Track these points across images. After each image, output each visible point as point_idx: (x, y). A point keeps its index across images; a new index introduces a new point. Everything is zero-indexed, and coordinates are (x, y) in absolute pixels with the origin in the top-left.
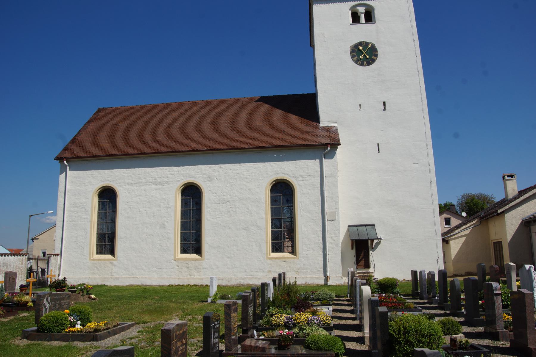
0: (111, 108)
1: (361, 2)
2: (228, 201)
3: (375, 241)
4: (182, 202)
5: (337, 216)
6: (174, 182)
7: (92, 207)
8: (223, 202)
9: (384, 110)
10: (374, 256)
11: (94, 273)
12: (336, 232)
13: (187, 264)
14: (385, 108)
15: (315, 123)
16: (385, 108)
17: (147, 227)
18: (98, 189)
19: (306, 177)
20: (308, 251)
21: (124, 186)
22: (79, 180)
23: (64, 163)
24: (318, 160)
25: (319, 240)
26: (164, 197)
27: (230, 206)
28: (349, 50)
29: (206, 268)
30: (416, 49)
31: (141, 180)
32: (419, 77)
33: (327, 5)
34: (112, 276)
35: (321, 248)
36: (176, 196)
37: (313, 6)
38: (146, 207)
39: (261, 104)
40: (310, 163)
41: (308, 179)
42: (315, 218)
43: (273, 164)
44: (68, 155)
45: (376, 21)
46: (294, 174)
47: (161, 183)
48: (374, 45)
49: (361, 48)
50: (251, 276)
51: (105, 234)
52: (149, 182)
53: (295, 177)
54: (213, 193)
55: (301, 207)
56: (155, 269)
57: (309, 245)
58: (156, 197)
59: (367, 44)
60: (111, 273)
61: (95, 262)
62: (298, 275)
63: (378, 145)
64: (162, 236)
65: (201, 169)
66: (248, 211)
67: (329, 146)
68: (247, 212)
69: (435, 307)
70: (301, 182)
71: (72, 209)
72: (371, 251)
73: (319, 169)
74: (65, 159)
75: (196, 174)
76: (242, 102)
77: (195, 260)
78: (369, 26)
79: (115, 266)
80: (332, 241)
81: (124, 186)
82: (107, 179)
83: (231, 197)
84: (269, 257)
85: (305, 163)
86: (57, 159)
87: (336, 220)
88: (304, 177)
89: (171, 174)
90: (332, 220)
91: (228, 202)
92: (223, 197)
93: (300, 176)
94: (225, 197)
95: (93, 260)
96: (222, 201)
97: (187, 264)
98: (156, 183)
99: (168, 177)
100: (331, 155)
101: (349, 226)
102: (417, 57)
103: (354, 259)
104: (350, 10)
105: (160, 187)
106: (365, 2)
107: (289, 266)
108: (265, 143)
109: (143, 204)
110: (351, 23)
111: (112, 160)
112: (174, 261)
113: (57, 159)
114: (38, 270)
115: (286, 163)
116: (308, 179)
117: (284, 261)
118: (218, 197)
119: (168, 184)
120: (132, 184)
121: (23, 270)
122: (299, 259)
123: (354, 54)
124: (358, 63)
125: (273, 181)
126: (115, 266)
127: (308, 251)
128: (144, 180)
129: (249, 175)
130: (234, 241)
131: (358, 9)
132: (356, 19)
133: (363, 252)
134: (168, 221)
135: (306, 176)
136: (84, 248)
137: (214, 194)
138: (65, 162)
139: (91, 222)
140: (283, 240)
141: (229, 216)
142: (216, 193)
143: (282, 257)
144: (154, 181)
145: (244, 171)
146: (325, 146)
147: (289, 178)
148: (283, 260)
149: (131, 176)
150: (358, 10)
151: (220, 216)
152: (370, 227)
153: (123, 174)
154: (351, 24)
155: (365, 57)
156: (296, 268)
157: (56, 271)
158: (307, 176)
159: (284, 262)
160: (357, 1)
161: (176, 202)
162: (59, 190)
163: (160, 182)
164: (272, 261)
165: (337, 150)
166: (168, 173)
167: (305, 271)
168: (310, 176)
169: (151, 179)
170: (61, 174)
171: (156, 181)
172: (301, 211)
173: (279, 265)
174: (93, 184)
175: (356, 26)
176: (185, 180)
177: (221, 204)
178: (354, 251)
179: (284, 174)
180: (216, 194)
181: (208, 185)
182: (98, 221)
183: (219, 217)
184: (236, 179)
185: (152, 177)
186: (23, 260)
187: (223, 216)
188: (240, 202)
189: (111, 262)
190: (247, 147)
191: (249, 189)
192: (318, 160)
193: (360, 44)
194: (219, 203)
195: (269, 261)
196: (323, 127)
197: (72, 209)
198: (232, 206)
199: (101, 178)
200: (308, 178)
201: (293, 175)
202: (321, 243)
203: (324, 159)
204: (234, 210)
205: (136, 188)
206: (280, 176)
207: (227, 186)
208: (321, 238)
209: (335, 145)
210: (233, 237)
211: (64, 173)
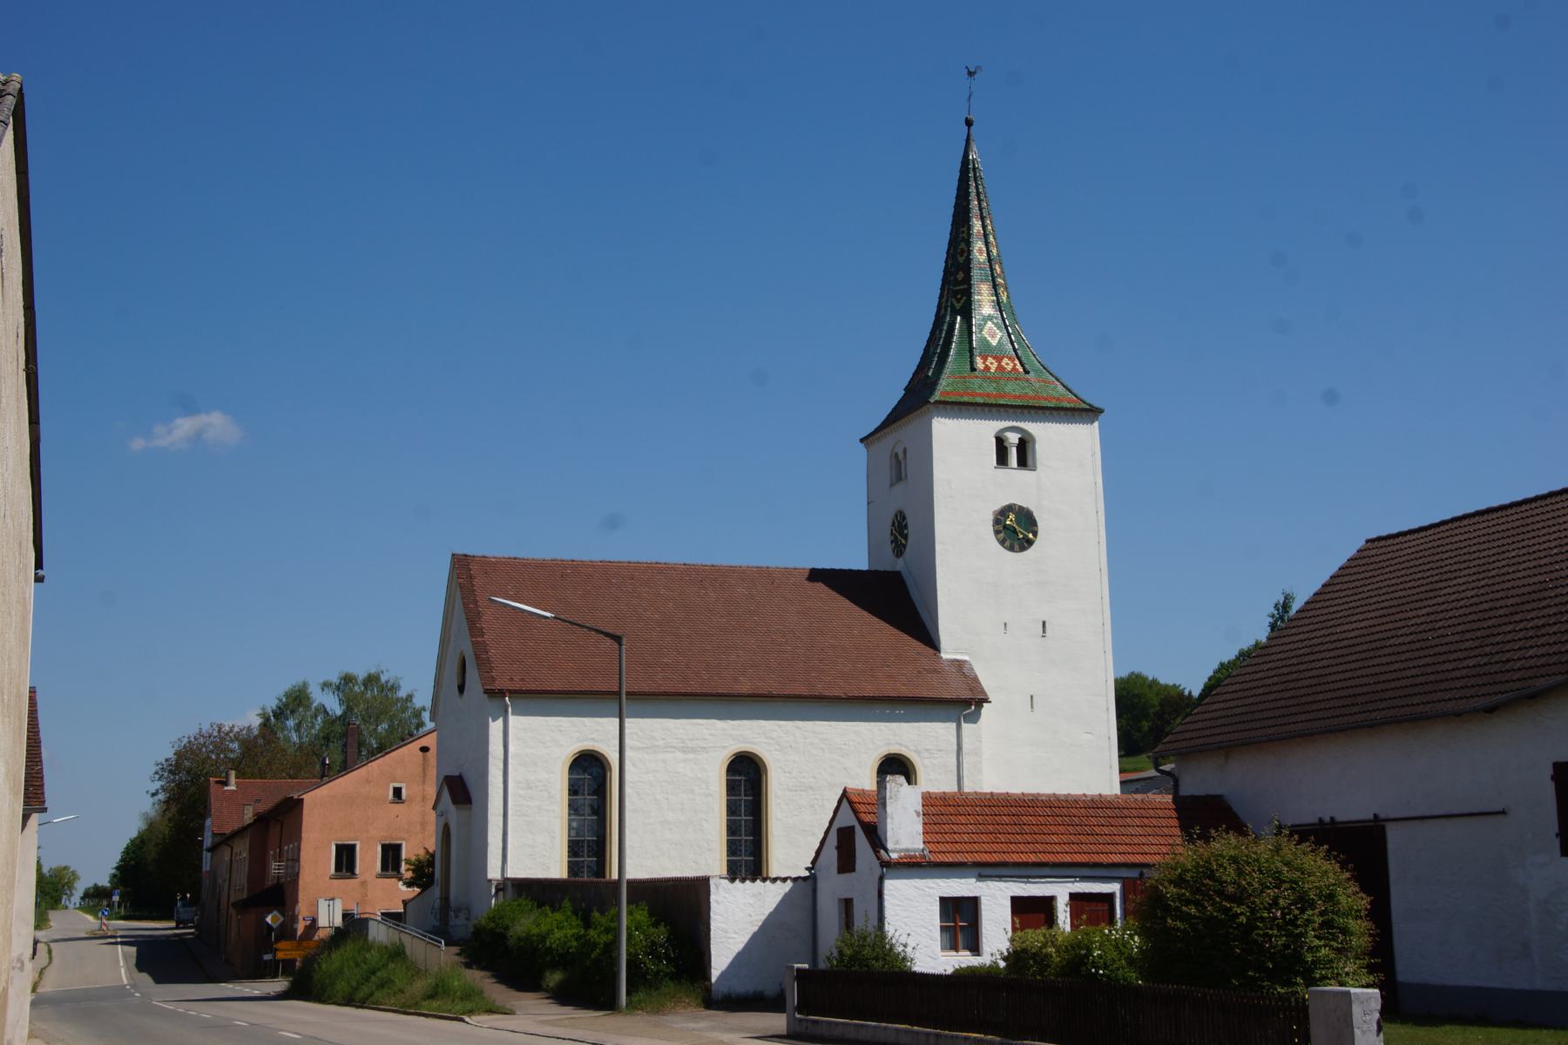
2: (811, 788)
9: (1043, 636)
14: (1044, 632)
15: (931, 651)
17: (670, 829)
23: (505, 701)
26: (700, 775)
28: (990, 518)
31: (656, 743)
37: (933, 421)
38: (667, 793)
47: (693, 750)
52: (675, 748)
53: (918, 752)
54: (785, 772)
63: (1032, 697)
71: (522, 792)
73: (954, 741)
74: (507, 694)
76: (767, 576)
78: (1024, 474)
82: (591, 737)
89: (712, 735)
92: (803, 780)
93: (926, 750)
98: (684, 750)
99: (705, 739)
100: (974, 718)
105: (691, 756)
108: (869, 690)
110: (995, 464)
119: (707, 752)
120: (639, 749)
128: (661, 743)
136: (548, 868)
137: (788, 775)
138: (507, 698)
142: (790, 773)
144: (681, 745)
146: (967, 703)
147: (908, 752)
149: (636, 733)
150: (1007, 438)
162: (490, 753)
163: (692, 748)
166: (705, 731)
168: (940, 751)
171: (684, 745)
174: (562, 745)
175: (1002, 472)
177: (799, 792)
179: (900, 744)
184: (823, 749)
185: (676, 739)
191: (845, 769)
192: (954, 725)
194: (796, 790)
196: (948, 660)
197: (522, 792)
198: (818, 797)
205: (646, 757)
206: (895, 749)
209: (981, 701)
211: (500, 721)
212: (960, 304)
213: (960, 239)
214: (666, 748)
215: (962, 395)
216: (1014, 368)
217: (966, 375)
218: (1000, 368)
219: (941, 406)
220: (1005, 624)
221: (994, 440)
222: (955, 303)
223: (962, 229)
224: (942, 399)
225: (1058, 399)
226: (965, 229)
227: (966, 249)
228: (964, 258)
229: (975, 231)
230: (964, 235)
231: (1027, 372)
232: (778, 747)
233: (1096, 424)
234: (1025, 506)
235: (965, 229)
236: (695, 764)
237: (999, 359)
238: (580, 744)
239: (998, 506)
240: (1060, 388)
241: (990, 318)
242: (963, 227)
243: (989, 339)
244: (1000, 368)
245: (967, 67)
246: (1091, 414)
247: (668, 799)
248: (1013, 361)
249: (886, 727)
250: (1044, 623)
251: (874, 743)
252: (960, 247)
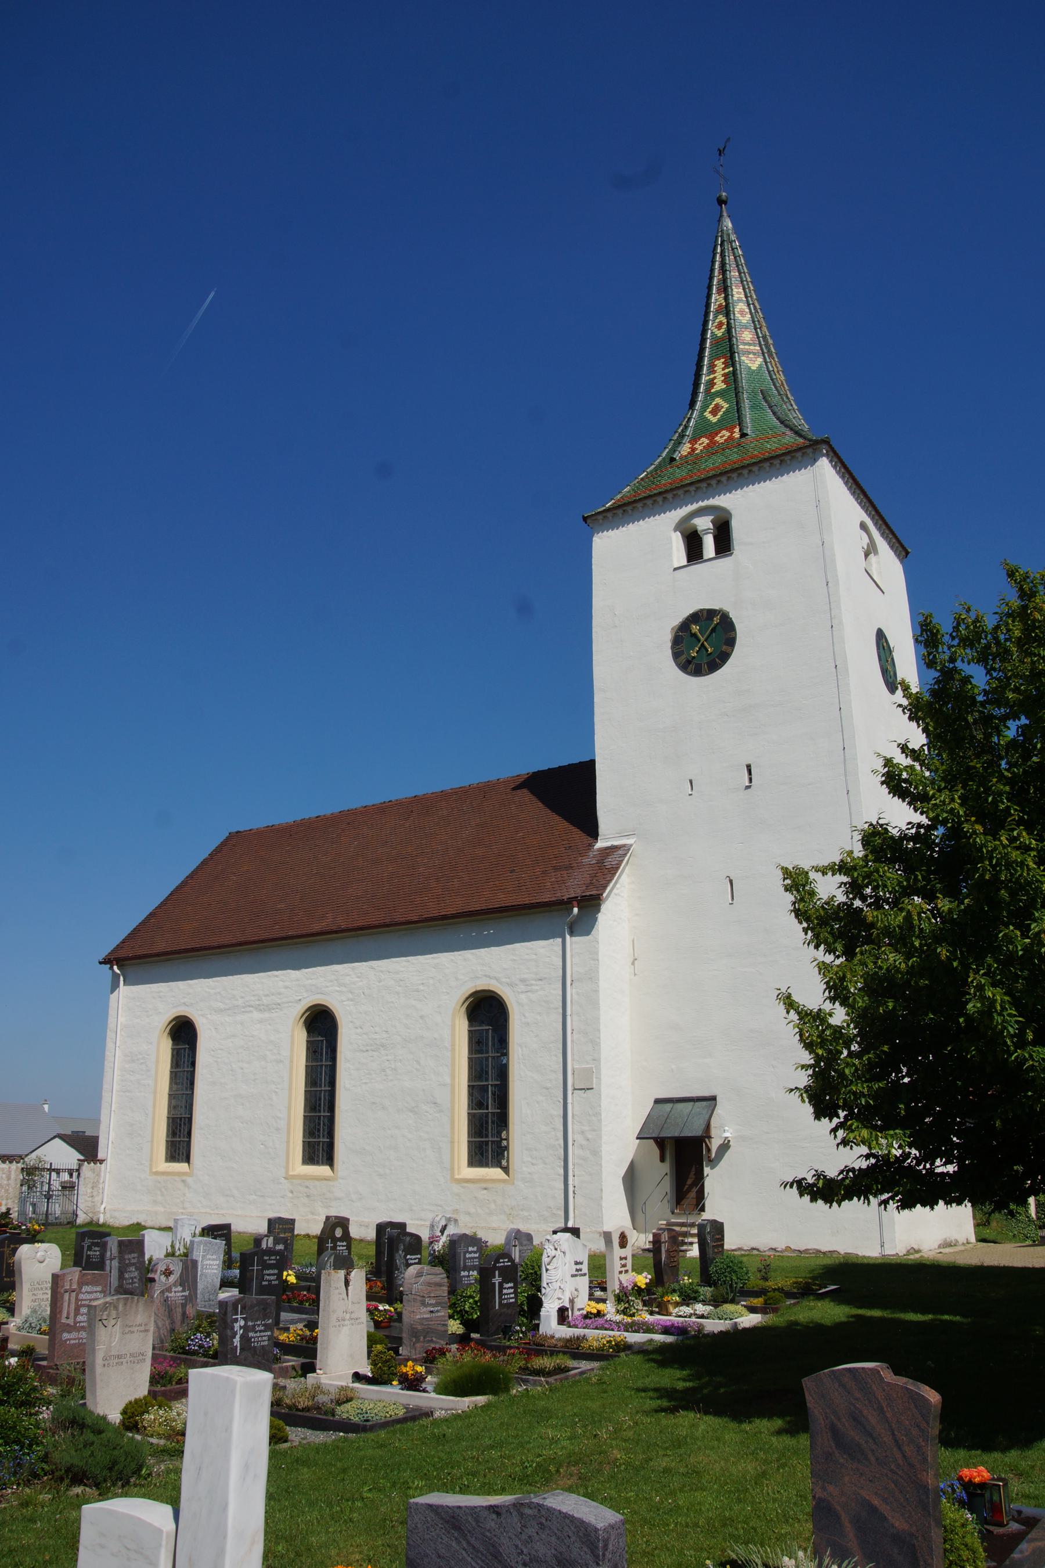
0: (250, 830)
1: (701, 504)
3: (715, 1144)
4: (308, 1049)
5: (596, 1078)
6: (290, 1004)
7: (157, 1061)
8: (372, 1048)
10: (714, 1179)
11: (155, 1202)
12: (594, 1118)
13: (307, 1187)
14: (750, 780)
16: (750, 780)
17: (243, 1104)
18: (167, 1022)
19: (533, 982)
20: (533, 1164)
21: (209, 1016)
22: (138, 1004)
24: (560, 940)
25: (557, 1140)
27: (386, 1058)
28: (668, 638)
29: (339, 1199)
33: (624, 529)
34: (184, 1208)
35: (560, 1159)
36: (292, 1036)
39: (525, 794)
40: (543, 948)
41: (536, 988)
42: (549, 1085)
43: (468, 954)
44: (122, 954)
46: (509, 978)
47: (269, 1008)
48: (728, 613)
49: (695, 628)
50: (421, 1220)
51: (181, 1118)
52: (249, 1006)
53: (511, 985)
55: (520, 1056)
56: (254, 1197)
57: (536, 1150)
58: (260, 1039)
59: (711, 613)
60: (183, 1202)
61: (159, 1178)
62: (512, 1223)
64: (268, 1124)
65: (336, 973)
66: (418, 1067)
67: (575, 903)
68: (416, 1069)
69: (839, 1326)
70: (523, 996)
72: (707, 1166)
74: (115, 962)
75: (328, 984)
76: (486, 790)
77: (322, 1180)
79: (189, 1187)
80: (584, 1142)
81: (209, 1016)
82: (182, 1001)
83: (388, 1035)
84: (457, 1177)
85: (531, 949)
86: (104, 962)
87: (592, 1089)
88: (528, 983)
89: (286, 987)
90: (584, 1089)
91: (382, 1049)
93: (522, 981)
94: (377, 1037)
95: (157, 1173)
96: (371, 1045)
97: (307, 1187)
98: (259, 1008)
99: (280, 994)
101: (658, 1101)
102: (833, 629)
103: (667, 1186)
104: (675, 530)
105: (267, 1015)
106: (711, 502)
107: (494, 1201)
109: (238, 1053)
111: (190, 959)
112: (286, 1181)
113: (104, 962)
114: (51, 1193)
115: (495, 950)
116: (536, 988)
117: (485, 1189)
118: (365, 1036)
119: (281, 1010)
121: (11, 1190)
122: (513, 1184)
123: (679, 648)
124: (689, 670)
125: (467, 995)
126: (189, 1187)
127: (533, 1164)
128: (240, 1002)
129: (423, 984)
130: (392, 1137)
131: (695, 523)
132: (694, 550)
133: (694, 1169)
134: (276, 1090)
135: (533, 980)
137: (359, 1031)
138: (115, 967)
139: (155, 1092)
140: (490, 1136)
141: (384, 1080)
142: (361, 1028)
143: (481, 1177)
144: (257, 1003)
145: (413, 976)
146: (565, 905)
147: (499, 985)
148: (484, 1185)
149: (219, 993)
150: (695, 526)
151: (368, 1081)
152: (704, 1103)
153: (207, 990)
155: (705, 652)
156: (507, 1205)
157: (95, 1194)
158: (536, 980)
159: (485, 1191)
161: (292, 1050)
162: (109, 1026)
163: (267, 1006)
164: (462, 1187)
165: (599, 911)
166: (281, 984)
167: (526, 1214)
168: (541, 980)
169: (253, 998)
170: (112, 992)
171: (260, 1002)
172: (522, 1066)
173: (475, 1197)
175: (697, 568)
176: (308, 999)
178: (666, 1168)
179: (489, 977)
180: (361, 1030)
181: (348, 1008)
182: (171, 1088)
183: (366, 1083)
184: (398, 993)
185: (254, 996)
186: (10, 1172)
187: (373, 1081)
188: (404, 1047)
189: (184, 1178)
190: (415, 919)
191: (422, 1017)
192: (560, 940)
193: (695, 617)
194: (367, 1051)
195: (456, 1188)
197: (127, 1066)
198: (389, 1057)
199: (173, 999)
200: (537, 985)
201: (508, 980)
202: (561, 1147)
203: (568, 937)
204: (393, 1066)
205: (227, 1019)
206: (482, 984)
207: (382, 1011)
208: (561, 1134)
210: (389, 1129)
214: (244, 1007)
220: (691, 782)
232: (350, 996)
236: (270, 1025)
238: (174, 1010)
239: (677, 620)
247: (242, 1069)
249: (472, 953)
250: (749, 768)
251: (457, 979)
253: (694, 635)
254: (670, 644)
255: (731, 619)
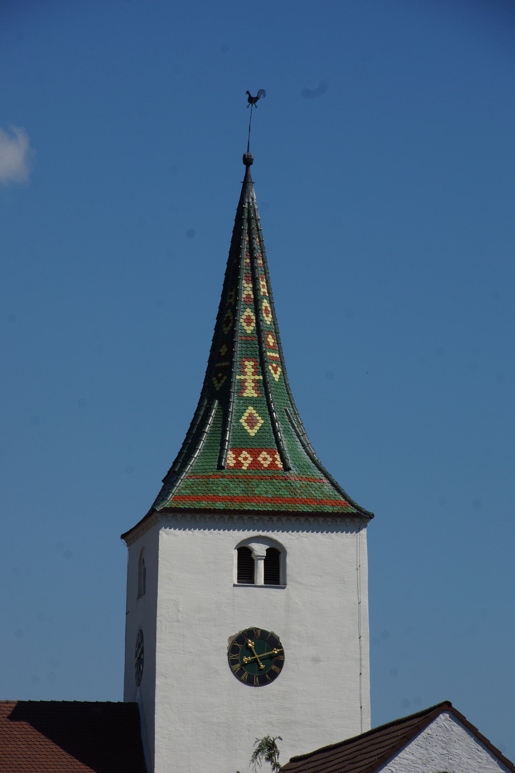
1: (261, 533)
28: (225, 645)
30: (363, 656)
32: (361, 721)
33: (190, 532)
45: (288, 582)
48: (279, 638)
106: (270, 534)
123: (234, 657)
154: (235, 585)
160: (253, 531)
212: (220, 385)
213: (227, 305)
215: (199, 499)
216: (273, 465)
217: (211, 474)
218: (255, 465)
219: (170, 515)
221: (235, 553)
222: (215, 382)
223: (230, 293)
224: (174, 505)
225: (321, 502)
226: (233, 293)
227: (231, 318)
228: (229, 328)
229: (244, 296)
230: (232, 300)
231: (287, 468)
233: (364, 532)
234: (269, 631)
235: (233, 293)
237: (255, 453)
239: (235, 632)
240: (328, 488)
241: (251, 401)
242: (232, 291)
243: (247, 428)
244: (255, 465)
245: (248, 92)
246: (357, 520)
248: (272, 456)
252: (227, 315)
253: (250, 648)
254: (227, 651)
255: (281, 644)
